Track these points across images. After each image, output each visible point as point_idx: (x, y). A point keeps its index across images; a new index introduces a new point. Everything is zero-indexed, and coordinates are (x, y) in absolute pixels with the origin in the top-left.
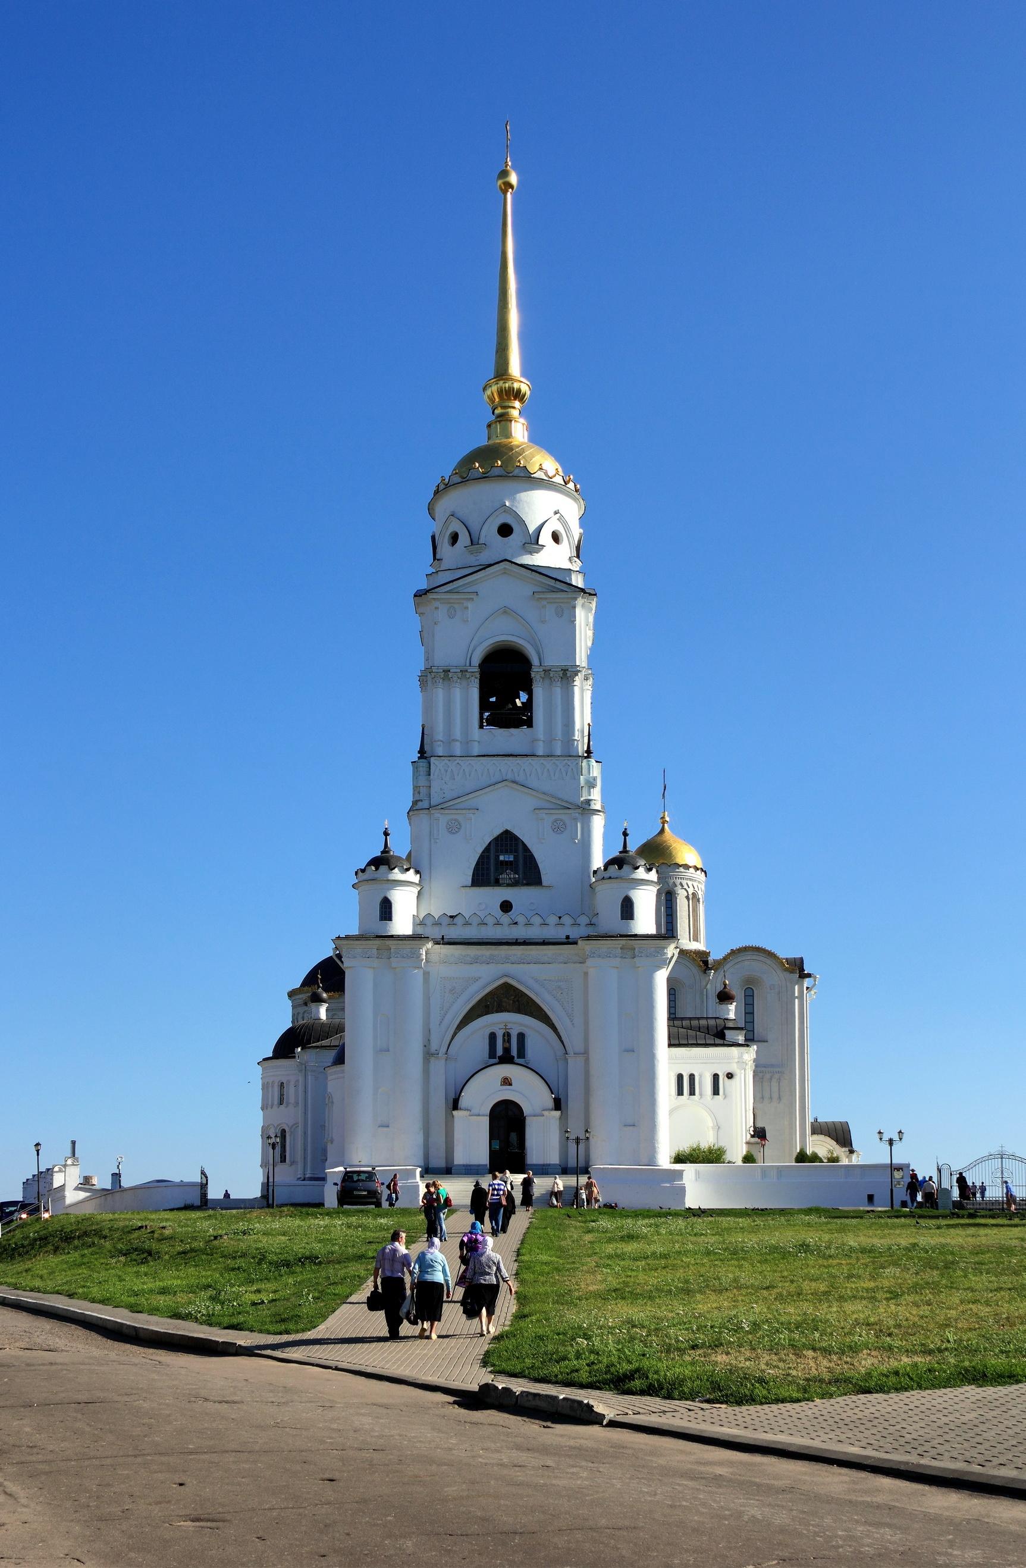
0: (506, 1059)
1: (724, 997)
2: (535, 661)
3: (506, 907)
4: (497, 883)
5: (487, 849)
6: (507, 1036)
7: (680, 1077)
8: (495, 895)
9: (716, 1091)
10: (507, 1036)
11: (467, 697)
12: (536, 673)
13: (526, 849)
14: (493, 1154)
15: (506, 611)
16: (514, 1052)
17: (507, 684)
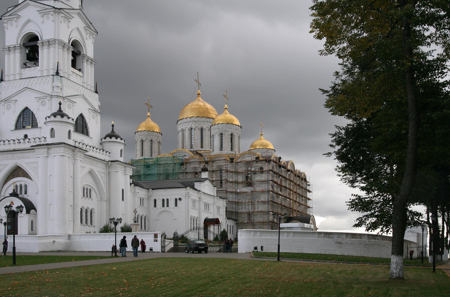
2: (40, 39)
7: (163, 200)
8: (21, 134)
9: (176, 205)
12: (39, 43)
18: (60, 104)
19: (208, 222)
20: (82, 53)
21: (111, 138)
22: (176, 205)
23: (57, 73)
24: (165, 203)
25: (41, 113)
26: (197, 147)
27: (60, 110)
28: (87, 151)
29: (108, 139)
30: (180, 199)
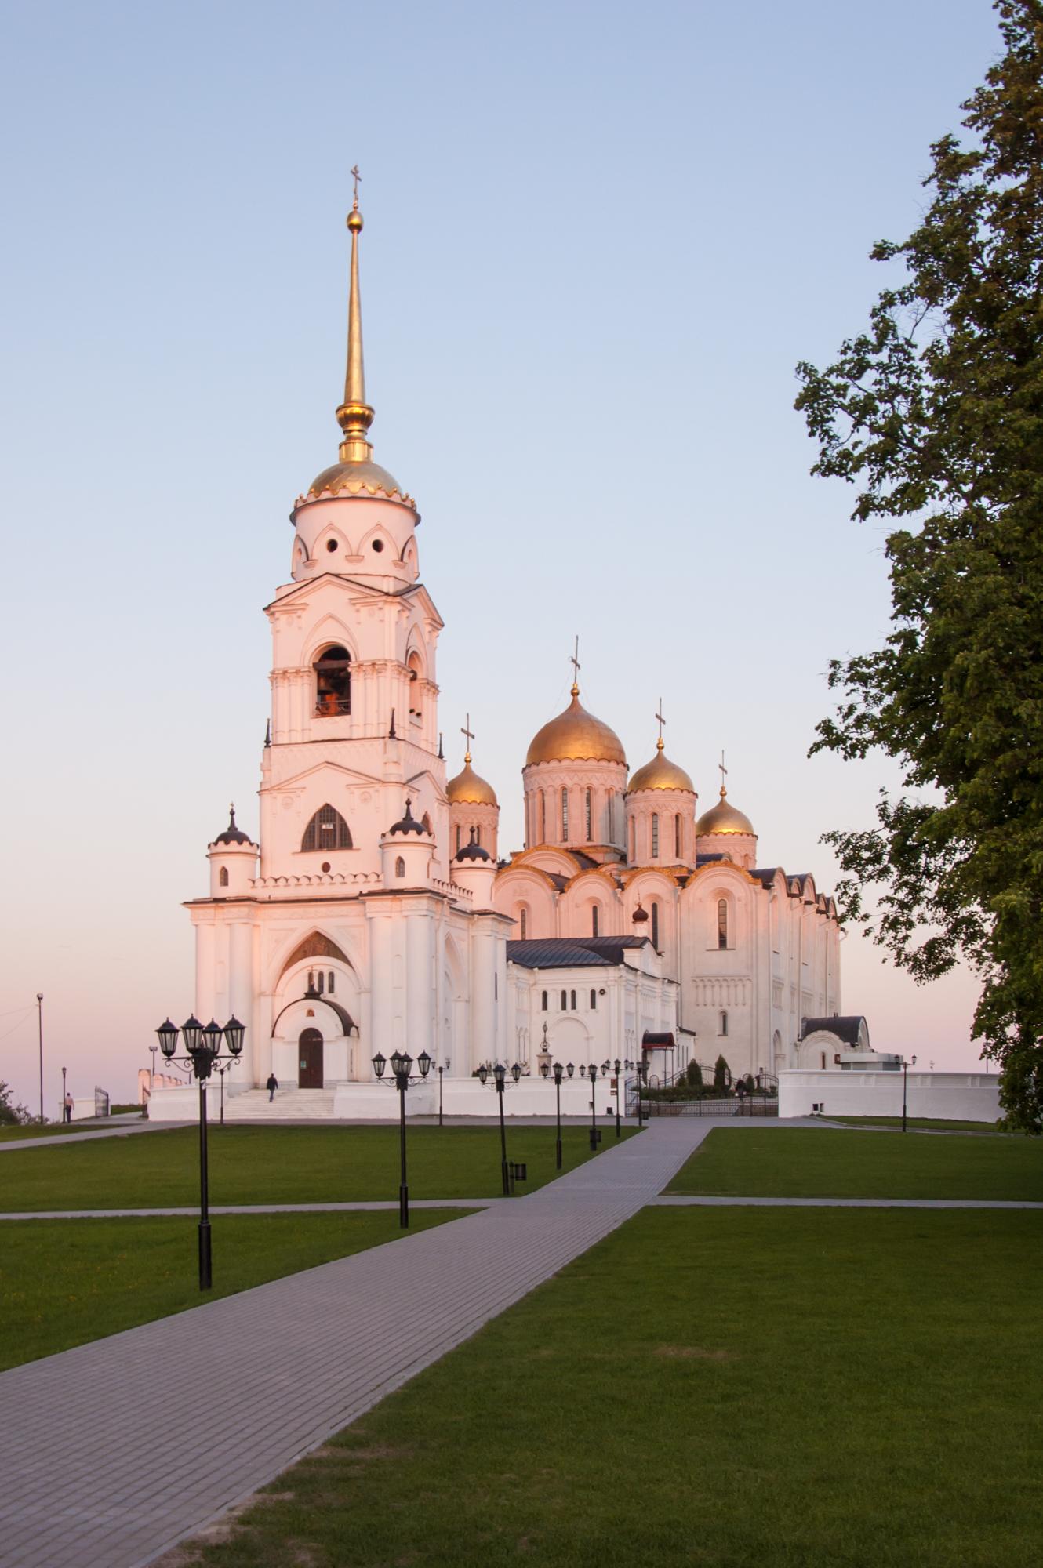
0: (312, 994)
1: (640, 917)
3: (326, 867)
4: (321, 848)
5: (313, 821)
6: (321, 975)
7: (564, 993)
9: (593, 1006)
10: (321, 975)
11: (304, 691)
12: (352, 668)
13: (342, 819)
14: (302, 1072)
15: (331, 617)
16: (316, 988)
17: (333, 677)
18: (408, 803)
19: (655, 1042)
20: (419, 676)
21: (473, 860)
22: (593, 1006)
23: (392, 733)
24: (568, 1000)
25: (367, 821)
26: (578, 840)
27: (408, 817)
28: (455, 901)
29: (467, 862)
30: (602, 992)
